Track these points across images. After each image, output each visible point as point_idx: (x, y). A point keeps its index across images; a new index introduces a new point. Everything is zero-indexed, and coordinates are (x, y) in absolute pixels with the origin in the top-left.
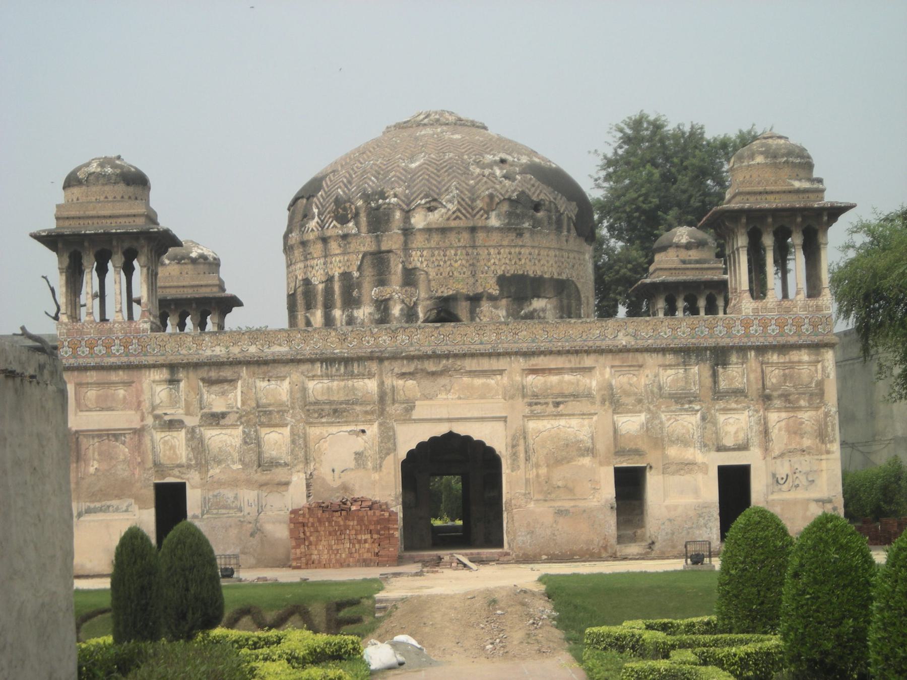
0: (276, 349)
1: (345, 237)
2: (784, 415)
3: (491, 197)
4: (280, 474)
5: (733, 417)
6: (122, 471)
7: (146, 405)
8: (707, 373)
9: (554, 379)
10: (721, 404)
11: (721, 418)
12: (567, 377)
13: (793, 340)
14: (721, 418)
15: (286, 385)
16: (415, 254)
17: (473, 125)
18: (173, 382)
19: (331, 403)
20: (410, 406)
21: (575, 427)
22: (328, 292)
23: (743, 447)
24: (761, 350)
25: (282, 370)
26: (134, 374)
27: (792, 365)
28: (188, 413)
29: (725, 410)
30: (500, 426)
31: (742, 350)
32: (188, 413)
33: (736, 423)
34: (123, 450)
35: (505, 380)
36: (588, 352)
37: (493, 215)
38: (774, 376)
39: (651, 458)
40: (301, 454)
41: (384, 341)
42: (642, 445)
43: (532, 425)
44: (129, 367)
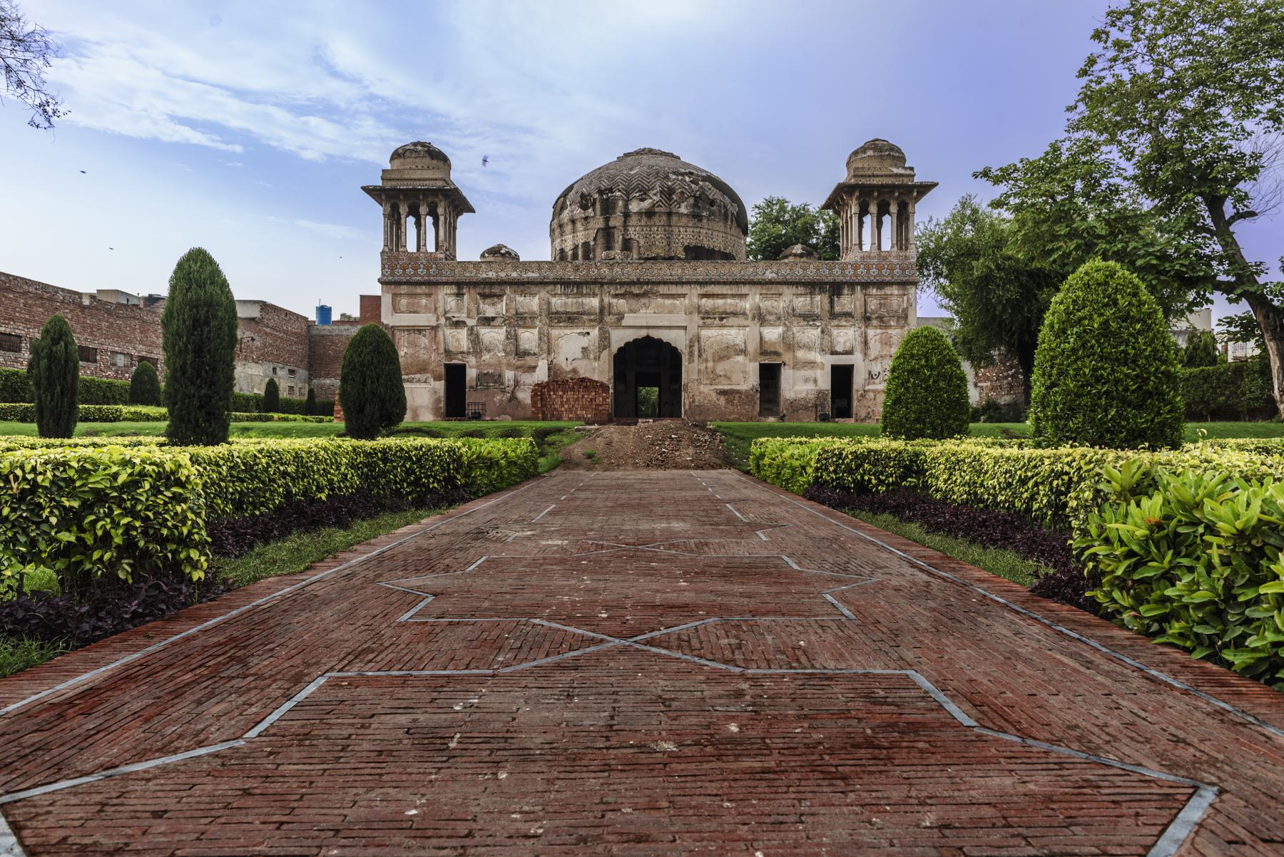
0: (530, 274)
1: (586, 218)
2: (879, 331)
3: (682, 193)
4: (530, 361)
5: (843, 331)
6: (423, 355)
7: (440, 310)
8: (826, 300)
9: (720, 302)
10: (835, 322)
11: (835, 332)
12: (729, 301)
13: (887, 279)
14: (835, 332)
15: (536, 300)
16: (631, 230)
17: (672, 155)
18: (459, 295)
19: (567, 313)
20: (621, 317)
21: (733, 335)
22: (575, 256)
23: (850, 352)
24: (865, 285)
25: (534, 289)
26: (433, 289)
27: (886, 297)
28: (469, 317)
29: (838, 326)
30: (682, 332)
31: (852, 285)
32: (469, 317)
33: (846, 335)
34: (424, 341)
35: (687, 301)
36: (744, 283)
37: (683, 205)
38: (873, 304)
39: (787, 357)
40: (545, 347)
41: (605, 271)
42: (781, 351)
43: (704, 333)
44: (429, 283)
